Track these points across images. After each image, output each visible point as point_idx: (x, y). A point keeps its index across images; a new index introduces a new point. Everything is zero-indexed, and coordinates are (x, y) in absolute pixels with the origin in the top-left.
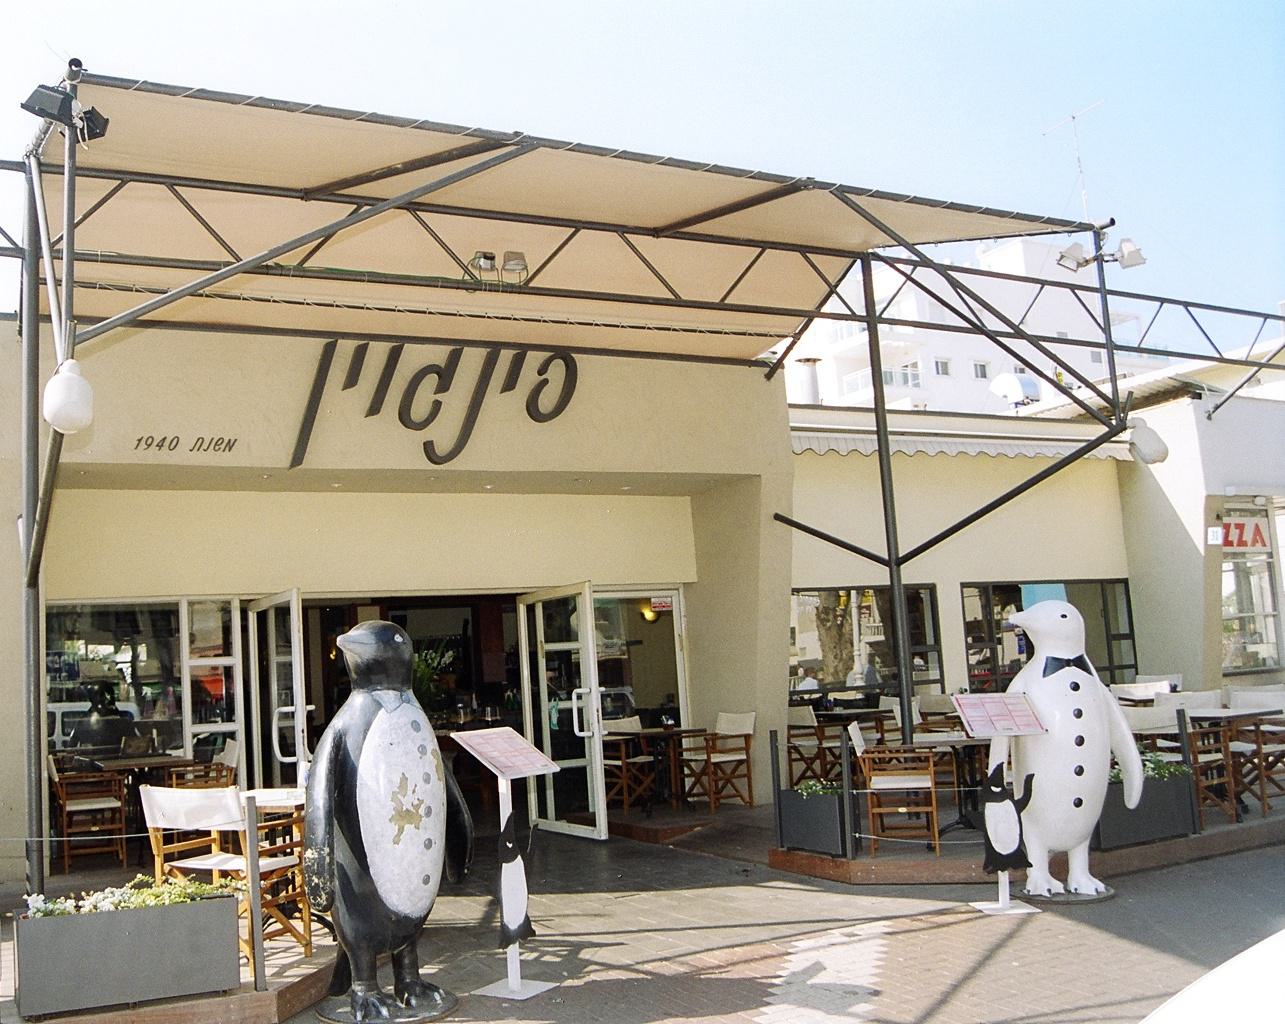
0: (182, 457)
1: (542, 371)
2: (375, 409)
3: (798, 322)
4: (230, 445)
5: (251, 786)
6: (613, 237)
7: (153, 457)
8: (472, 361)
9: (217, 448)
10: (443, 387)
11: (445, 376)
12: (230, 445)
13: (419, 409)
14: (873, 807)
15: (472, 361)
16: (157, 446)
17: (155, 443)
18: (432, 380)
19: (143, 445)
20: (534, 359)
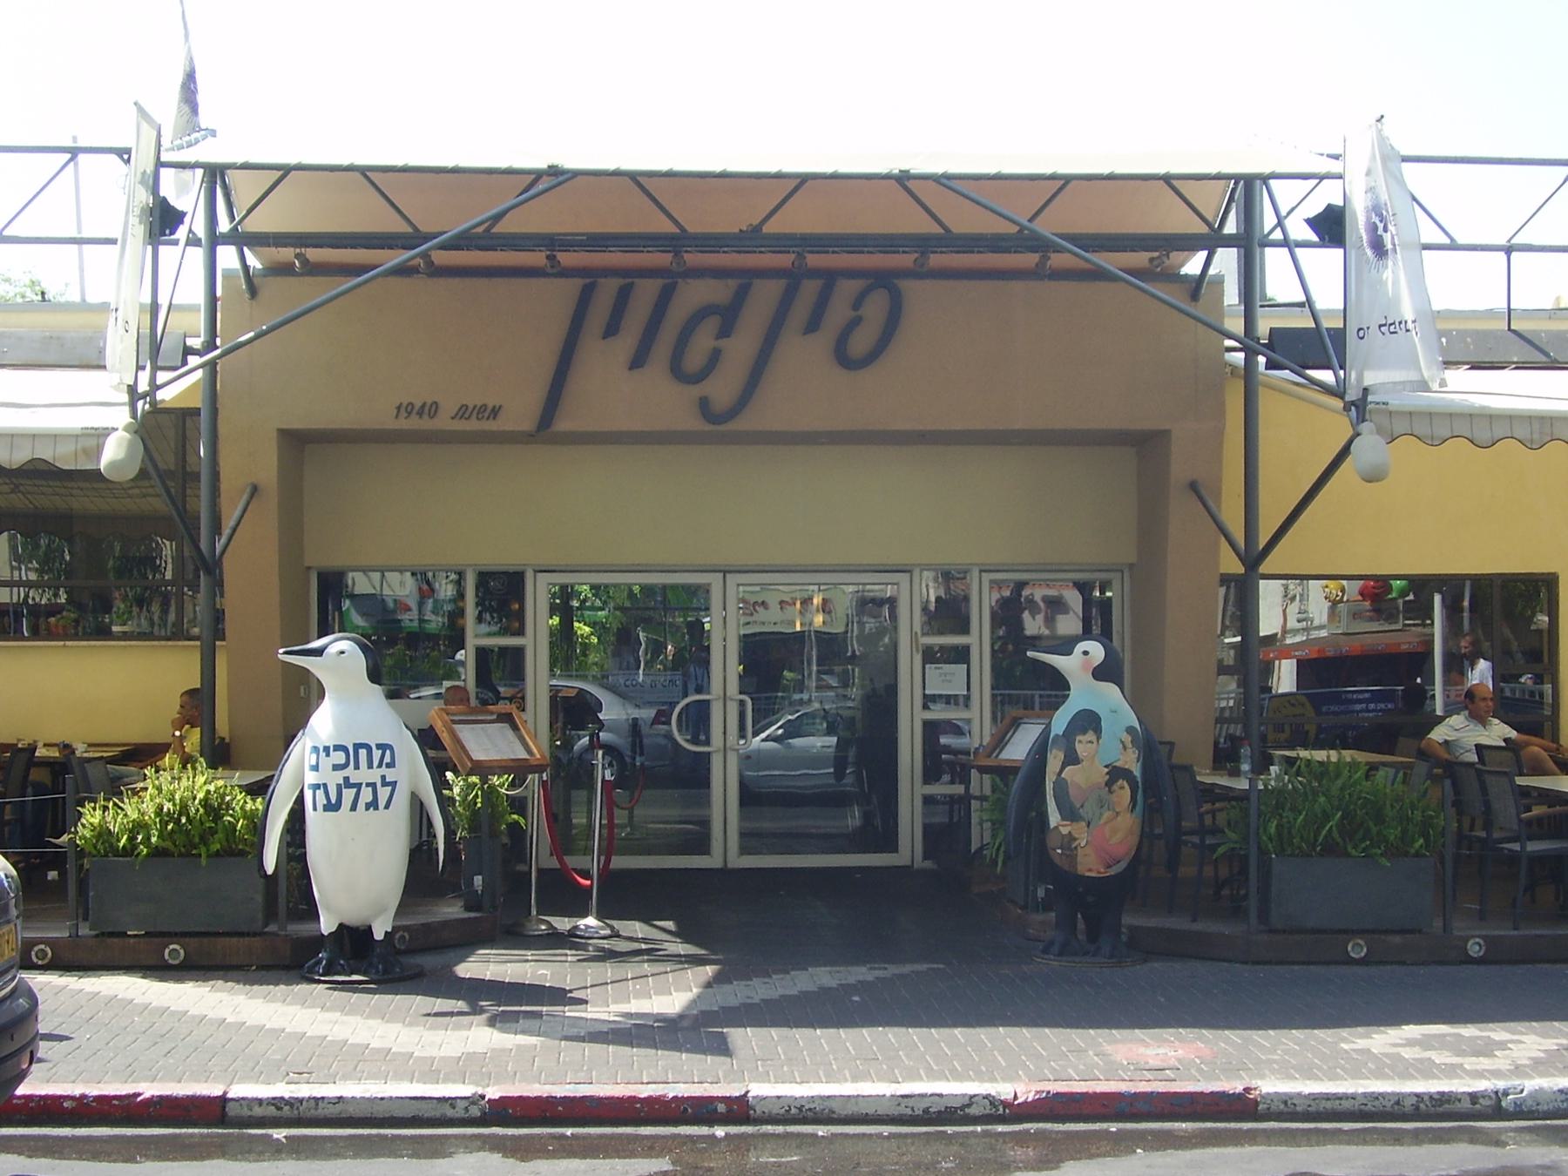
0: (444, 422)
1: (857, 304)
2: (637, 362)
3: (1183, 186)
4: (495, 412)
5: (810, 631)
6: (1461, 241)
7: (414, 423)
8: (766, 294)
9: (480, 416)
10: (725, 332)
11: (728, 317)
12: (495, 412)
13: (695, 358)
14: (1041, 696)
15: (766, 294)
16: (418, 413)
17: (415, 411)
18: (711, 325)
19: (403, 413)
20: (847, 289)
